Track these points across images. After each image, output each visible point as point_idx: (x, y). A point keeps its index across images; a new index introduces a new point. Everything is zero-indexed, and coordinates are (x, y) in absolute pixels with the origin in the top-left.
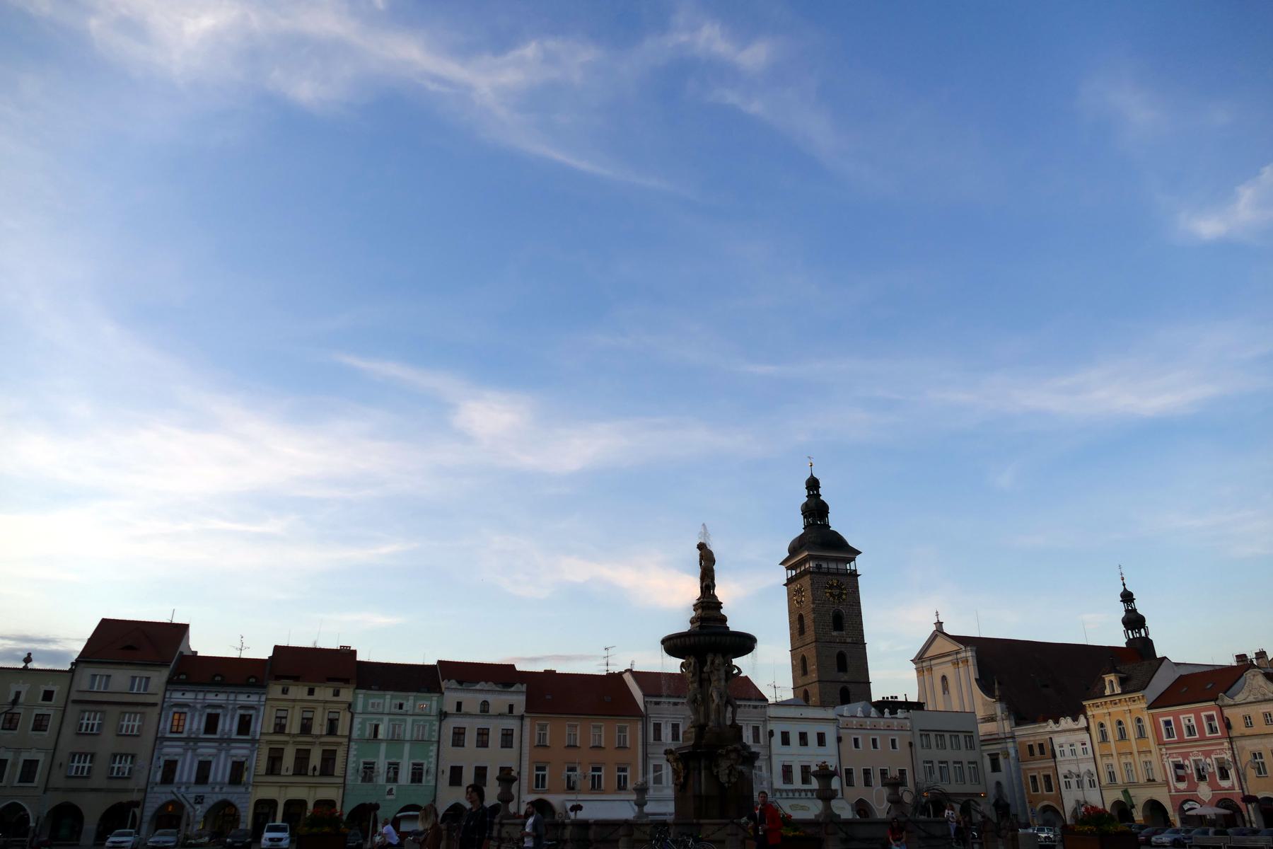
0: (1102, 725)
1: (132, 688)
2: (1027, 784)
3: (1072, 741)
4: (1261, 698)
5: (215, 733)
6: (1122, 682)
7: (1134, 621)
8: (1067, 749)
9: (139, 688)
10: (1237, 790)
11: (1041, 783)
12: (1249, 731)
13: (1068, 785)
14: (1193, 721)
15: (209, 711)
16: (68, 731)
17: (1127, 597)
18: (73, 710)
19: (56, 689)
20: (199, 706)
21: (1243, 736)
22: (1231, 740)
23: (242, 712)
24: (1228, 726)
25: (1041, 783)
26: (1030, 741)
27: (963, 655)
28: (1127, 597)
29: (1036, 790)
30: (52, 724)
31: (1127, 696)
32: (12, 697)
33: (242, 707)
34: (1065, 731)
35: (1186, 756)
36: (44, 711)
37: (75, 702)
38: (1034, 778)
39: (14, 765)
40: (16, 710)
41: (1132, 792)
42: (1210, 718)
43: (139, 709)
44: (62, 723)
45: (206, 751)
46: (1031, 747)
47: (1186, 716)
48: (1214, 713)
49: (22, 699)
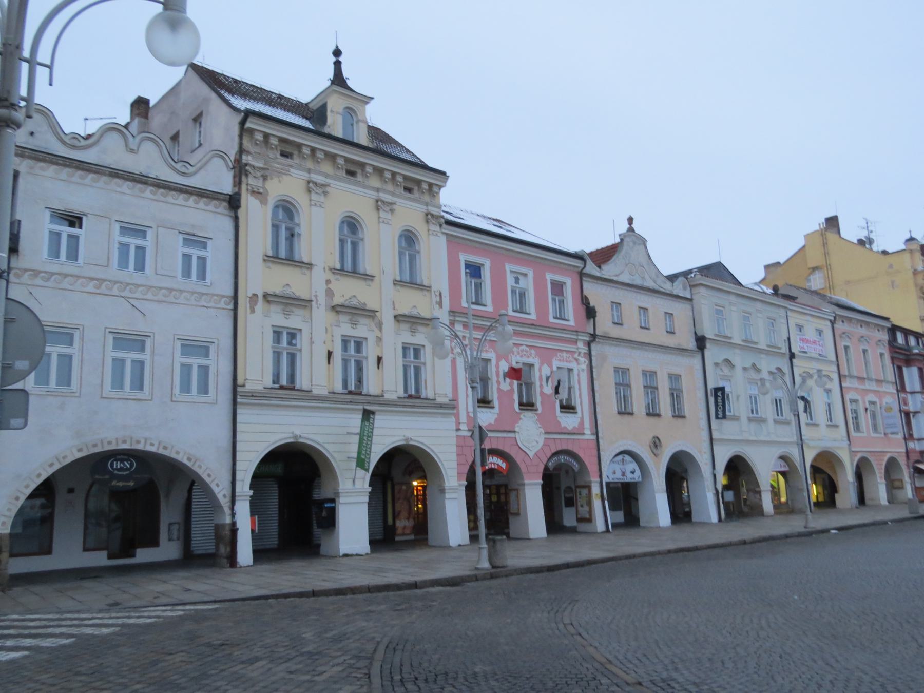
0: (287, 209)
4: (638, 281)
10: (588, 435)
12: (615, 332)
21: (607, 338)
24: (591, 313)
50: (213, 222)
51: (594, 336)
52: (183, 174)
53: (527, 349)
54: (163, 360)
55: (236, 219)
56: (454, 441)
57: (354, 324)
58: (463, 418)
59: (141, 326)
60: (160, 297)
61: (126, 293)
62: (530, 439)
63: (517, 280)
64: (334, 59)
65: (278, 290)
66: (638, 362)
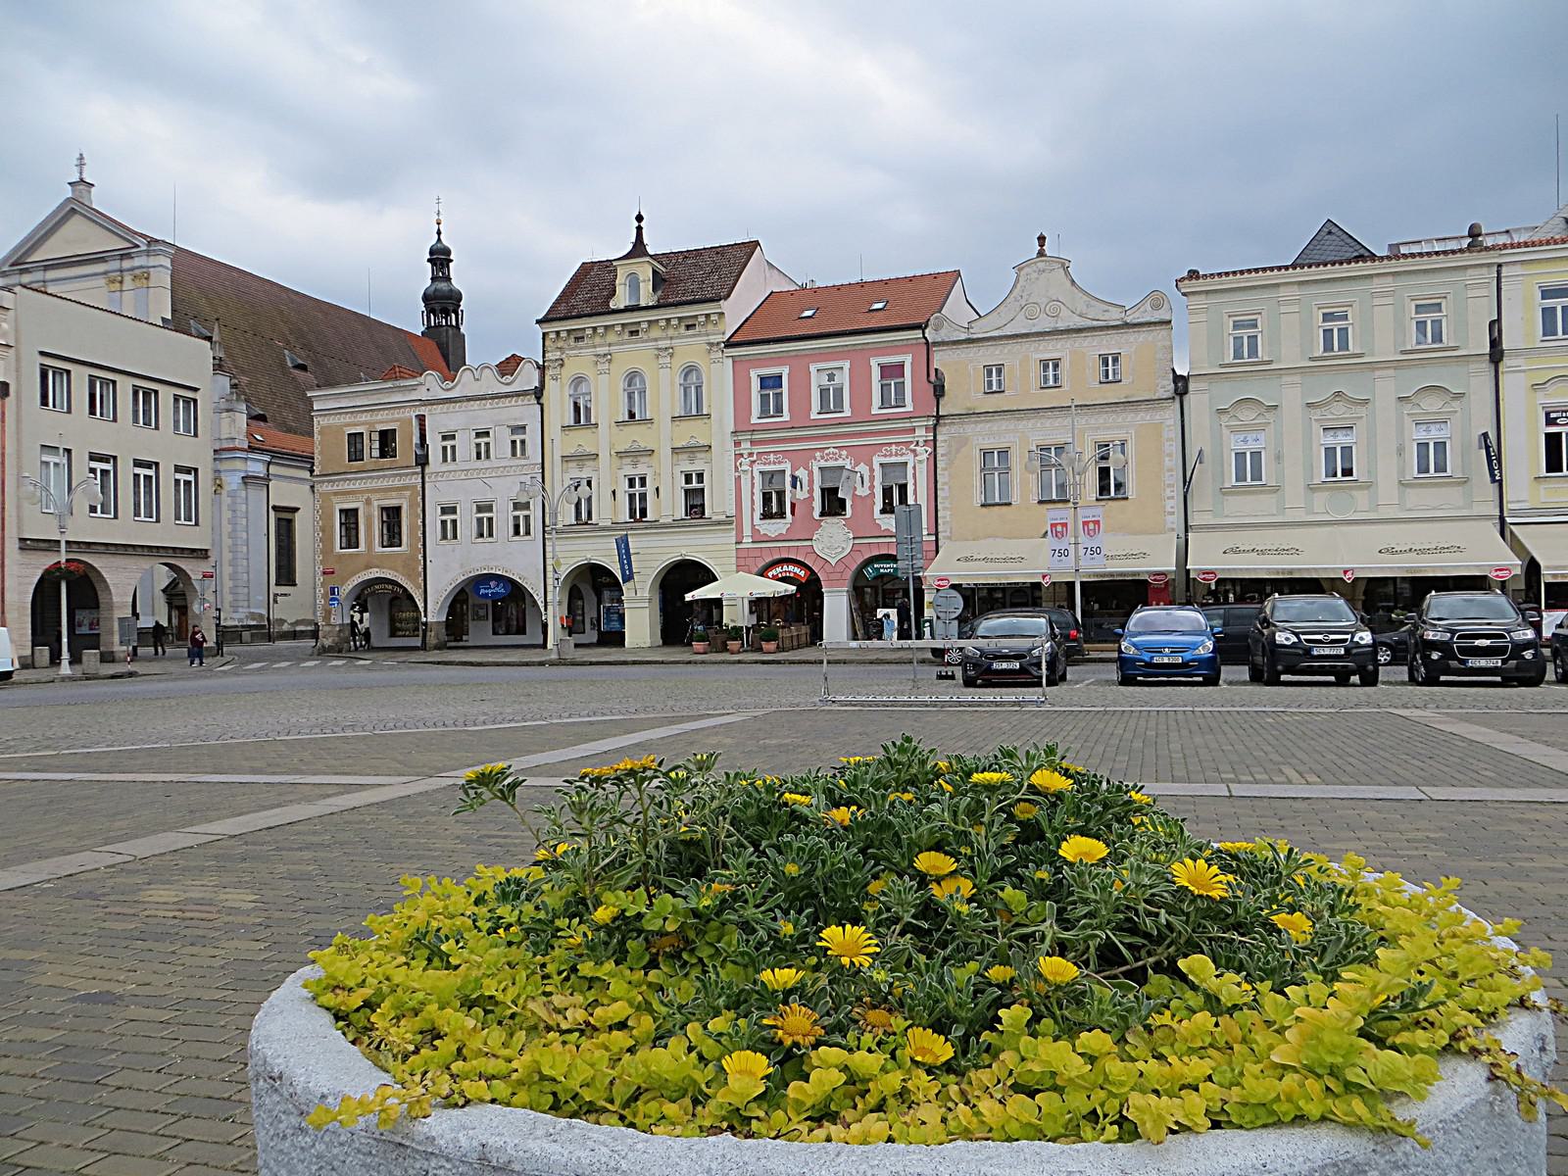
2: (327, 530)
3: (482, 427)
6: (658, 280)
7: (442, 302)
8: (465, 444)
11: (371, 528)
13: (449, 531)
14: (843, 379)
17: (440, 258)
22: (938, 417)
24: (939, 391)
25: (371, 528)
26: (360, 424)
27: (137, 262)
28: (440, 258)
29: (351, 540)
31: (673, 313)
34: (469, 399)
35: (802, 458)
38: (350, 516)
41: (633, 544)
42: (892, 371)
46: (355, 439)
47: (827, 371)
48: (908, 360)
50: (525, 412)
51: (938, 417)
52: (508, 384)
53: (836, 451)
54: (503, 518)
55: (542, 405)
56: (734, 553)
57: (635, 465)
58: (747, 531)
59: (489, 496)
60: (499, 473)
61: (481, 475)
62: (834, 545)
63: (831, 378)
64: (637, 224)
65: (572, 451)
66: (1023, 438)
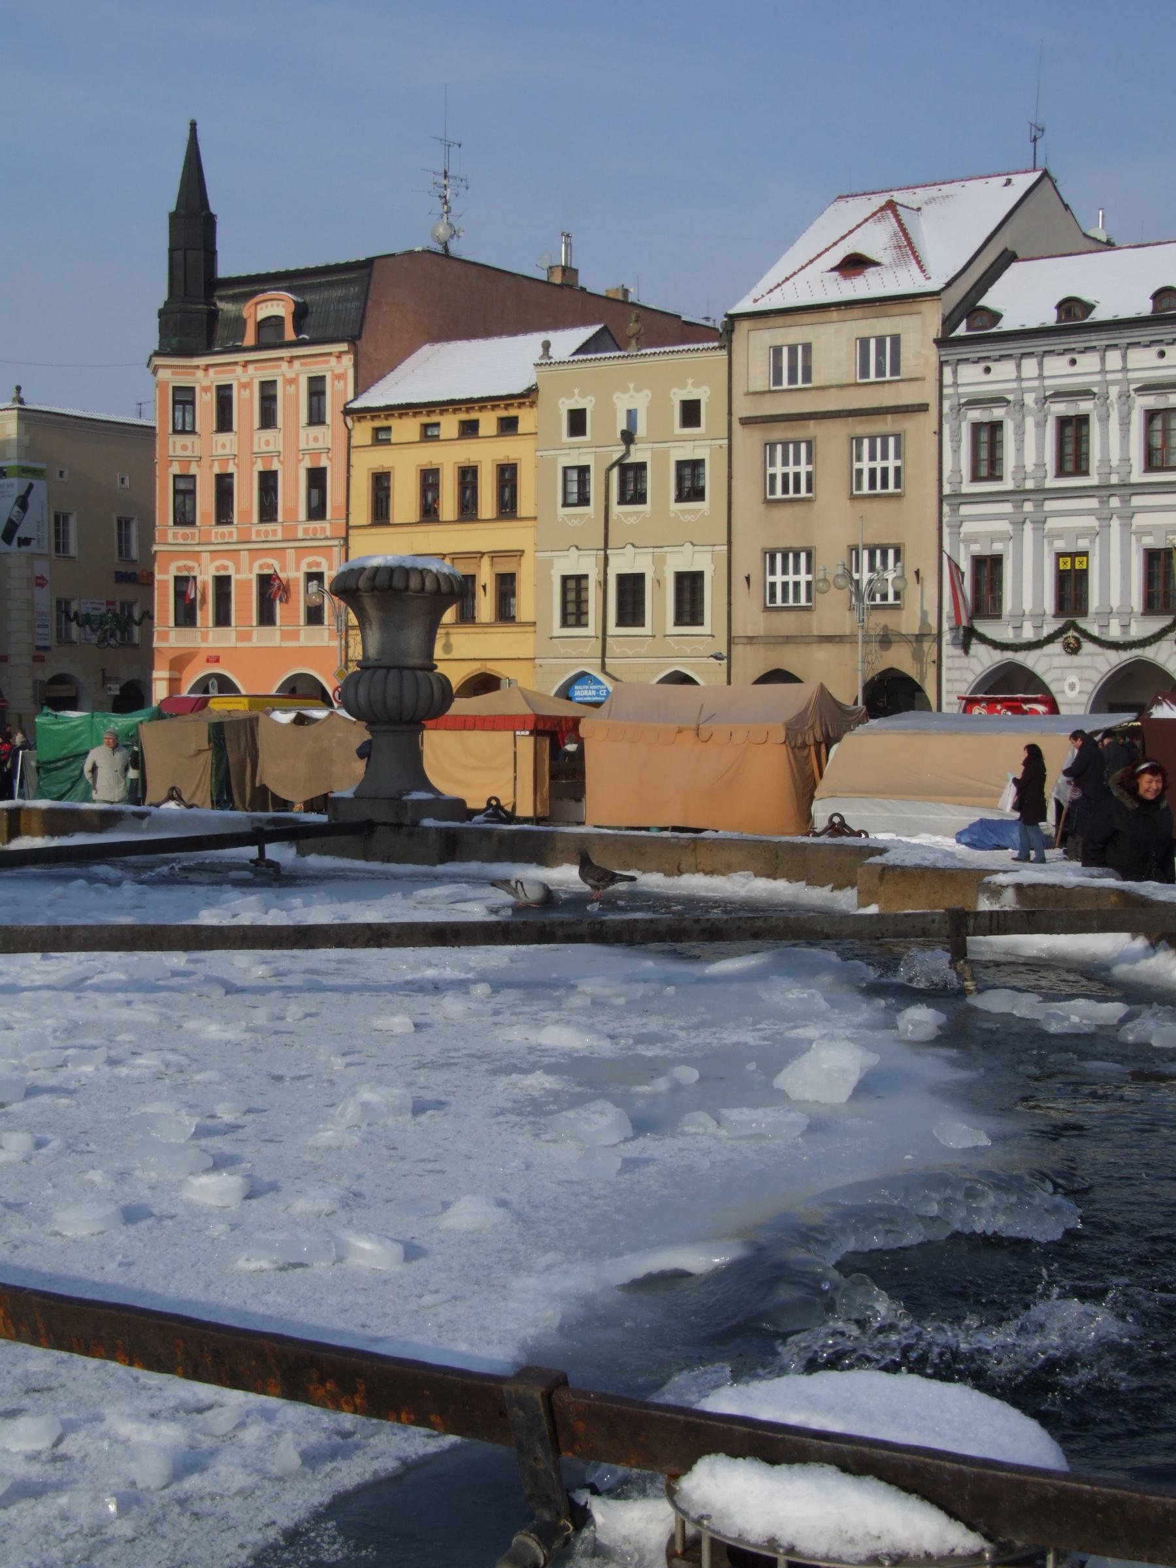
1: (865, 372)
5: (1086, 473)
9: (880, 372)
15: (1061, 408)
16: (747, 494)
18: (748, 442)
19: (701, 393)
20: (1029, 399)
23: (1151, 401)
30: (712, 480)
32: (622, 425)
33: (1147, 388)
36: (688, 453)
37: (746, 422)
39: (658, 582)
40: (635, 457)
43: (888, 424)
44: (730, 478)
45: (1071, 521)
49: (641, 431)
